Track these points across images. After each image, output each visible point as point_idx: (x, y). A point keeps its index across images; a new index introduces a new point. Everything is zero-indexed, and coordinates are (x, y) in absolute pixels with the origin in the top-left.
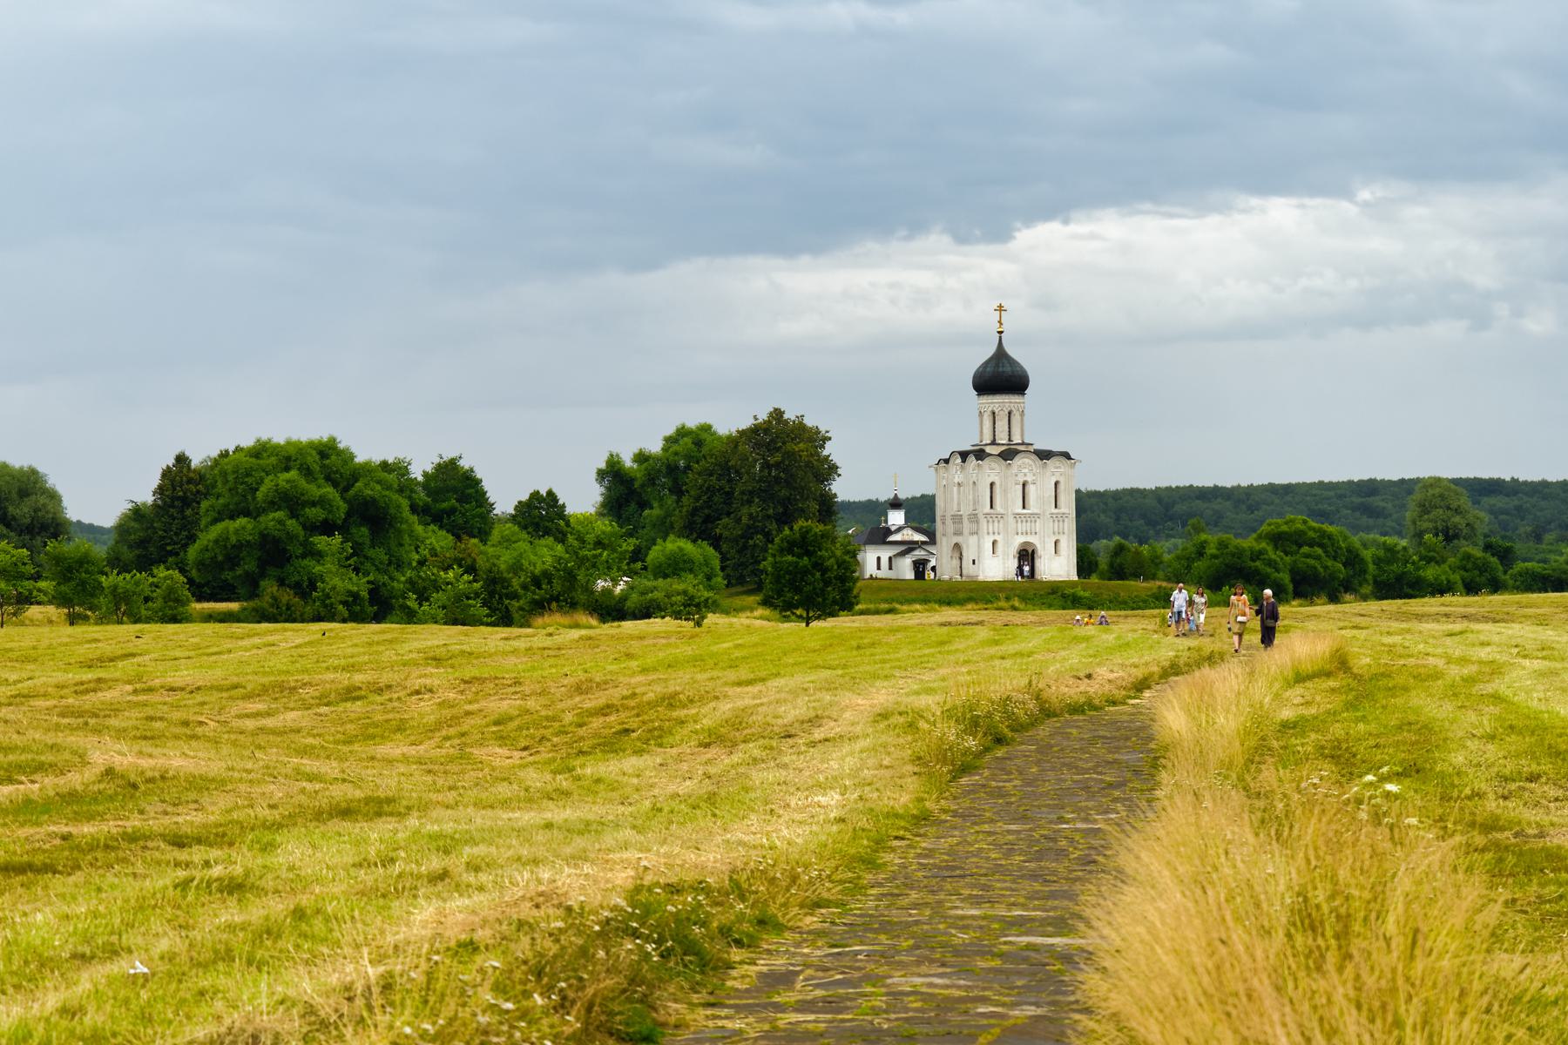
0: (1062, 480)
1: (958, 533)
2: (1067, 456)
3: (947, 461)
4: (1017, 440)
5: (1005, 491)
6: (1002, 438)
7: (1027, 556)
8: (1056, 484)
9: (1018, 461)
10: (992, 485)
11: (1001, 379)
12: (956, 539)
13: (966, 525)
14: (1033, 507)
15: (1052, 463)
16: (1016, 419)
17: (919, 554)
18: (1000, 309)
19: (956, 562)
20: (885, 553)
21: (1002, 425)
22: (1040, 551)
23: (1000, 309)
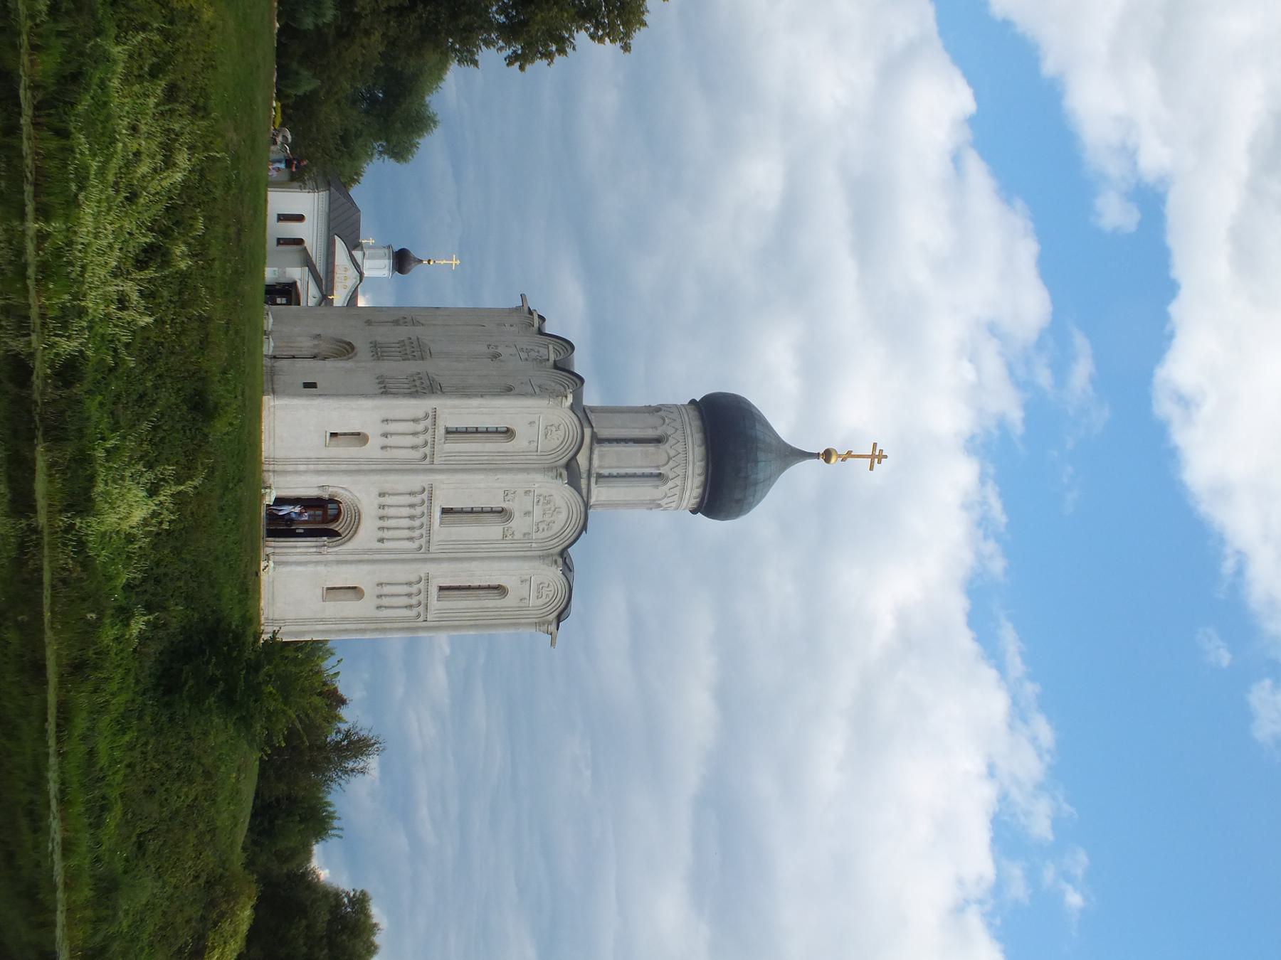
0: (510, 601)
1: (379, 351)
3: (540, 332)
4: (599, 493)
8: (500, 590)
10: (508, 433)
11: (731, 451)
13: (397, 368)
15: (553, 574)
16: (647, 491)
17: (309, 294)
18: (877, 456)
19: (306, 344)
20: (310, 232)
21: (636, 458)
23: (877, 456)
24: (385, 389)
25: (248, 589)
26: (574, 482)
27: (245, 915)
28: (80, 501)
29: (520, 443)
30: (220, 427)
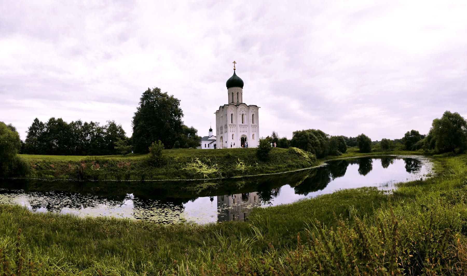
0: (254, 114)
2: (256, 106)
4: (240, 102)
5: (237, 117)
6: (235, 101)
7: (243, 140)
8: (253, 115)
9: (240, 107)
10: (232, 115)
12: (221, 135)
13: (224, 130)
14: (245, 123)
16: (240, 95)
18: (234, 62)
21: (235, 97)
22: (248, 138)
23: (234, 62)
24: (226, 132)
25: (252, 150)
26: (238, 105)
27: (295, 148)
28: (240, 172)
29: (233, 113)
30: (231, 154)
